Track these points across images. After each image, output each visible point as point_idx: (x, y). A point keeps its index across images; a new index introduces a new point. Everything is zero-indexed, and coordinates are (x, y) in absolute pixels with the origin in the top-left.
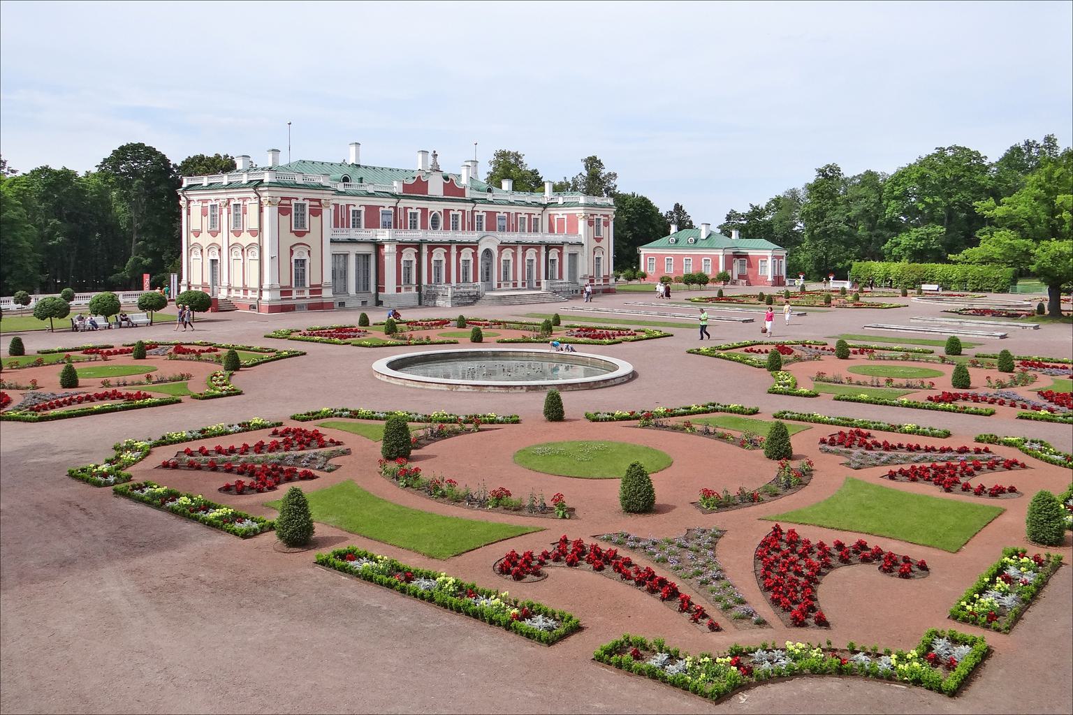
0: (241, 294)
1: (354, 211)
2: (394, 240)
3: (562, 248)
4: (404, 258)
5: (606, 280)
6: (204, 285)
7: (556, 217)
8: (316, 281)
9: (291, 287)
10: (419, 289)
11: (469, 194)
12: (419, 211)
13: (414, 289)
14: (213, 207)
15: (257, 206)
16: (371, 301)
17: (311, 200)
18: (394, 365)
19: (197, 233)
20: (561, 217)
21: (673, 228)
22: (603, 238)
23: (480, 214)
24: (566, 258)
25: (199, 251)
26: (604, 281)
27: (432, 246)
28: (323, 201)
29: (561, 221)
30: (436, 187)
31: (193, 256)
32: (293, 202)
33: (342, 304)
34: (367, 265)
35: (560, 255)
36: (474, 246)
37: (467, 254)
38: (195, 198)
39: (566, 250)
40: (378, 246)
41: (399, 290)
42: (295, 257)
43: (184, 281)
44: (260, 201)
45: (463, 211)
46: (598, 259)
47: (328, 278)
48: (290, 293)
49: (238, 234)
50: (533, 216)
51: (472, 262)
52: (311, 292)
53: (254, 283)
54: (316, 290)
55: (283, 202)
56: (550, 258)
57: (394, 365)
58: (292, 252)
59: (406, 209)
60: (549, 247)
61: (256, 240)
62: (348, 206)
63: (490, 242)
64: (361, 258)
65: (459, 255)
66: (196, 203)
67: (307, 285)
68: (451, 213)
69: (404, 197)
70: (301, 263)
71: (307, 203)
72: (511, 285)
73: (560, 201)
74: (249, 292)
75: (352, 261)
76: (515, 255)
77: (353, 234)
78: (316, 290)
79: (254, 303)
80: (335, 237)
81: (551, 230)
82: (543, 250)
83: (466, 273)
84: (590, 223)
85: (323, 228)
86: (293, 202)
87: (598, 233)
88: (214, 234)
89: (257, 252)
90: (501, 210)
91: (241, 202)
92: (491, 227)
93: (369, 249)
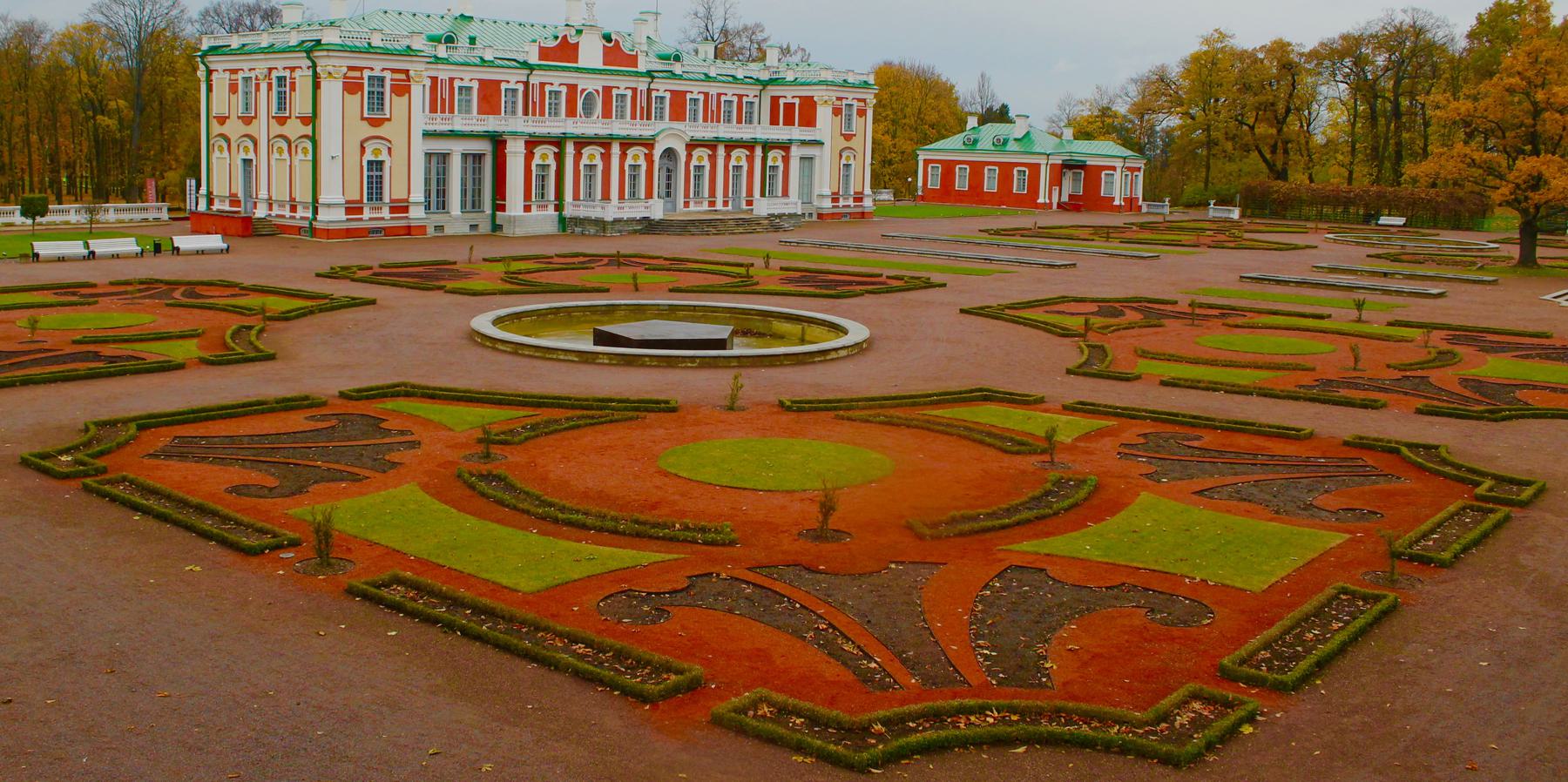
0: (287, 213)
1: (461, 88)
2: (522, 134)
4: (537, 161)
5: (859, 198)
6: (234, 201)
7: (782, 101)
8: (400, 194)
9: (361, 201)
10: (559, 208)
11: (642, 66)
12: (564, 90)
13: (551, 208)
14: (246, 80)
15: (310, 81)
16: (485, 228)
17: (394, 71)
18: (497, 322)
19: (222, 120)
20: (790, 100)
21: (972, 122)
23: (660, 94)
24: (795, 164)
25: (225, 145)
26: (856, 200)
27: (581, 143)
28: (412, 73)
29: (789, 107)
30: (591, 53)
31: (216, 154)
32: (366, 74)
33: (439, 228)
34: (478, 171)
35: (786, 160)
36: (648, 144)
37: (636, 155)
38: (220, 67)
39: (795, 152)
40: (498, 142)
41: (527, 208)
42: (369, 156)
43: (203, 190)
44: (315, 73)
46: (847, 166)
47: (418, 195)
48: (360, 210)
49: (282, 121)
50: (745, 99)
51: (644, 168)
52: (393, 210)
53: (303, 194)
54: (400, 207)
55: (351, 74)
56: (770, 163)
57: (497, 322)
58: (363, 149)
59: (542, 85)
60: (768, 146)
61: (308, 130)
62: (452, 80)
63: (670, 134)
64: (470, 160)
66: (222, 75)
67: (386, 199)
68: (615, 92)
69: (540, 67)
70: (376, 165)
71: (388, 75)
72: (705, 207)
73: (790, 78)
74: (299, 208)
75: (456, 165)
76: (713, 159)
77: (459, 123)
78: (400, 207)
79: (306, 224)
80: (431, 128)
81: (774, 121)
82: (759, 151)
83: (634, 186)
84: (837, 111)
85: (413, 115)
86: (366, 74)
87: (849, 126)
88: (247, 121)
89: (309, 145)
90: (695, 91)
91: (287, 73)
92: (678, 114)
93: (484, 147)
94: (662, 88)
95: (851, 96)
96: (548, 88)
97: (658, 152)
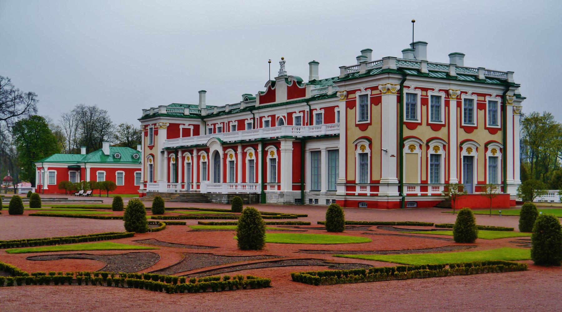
3: (280, 143)
11: (308, 96)
12: (270, 119)
22: (370, 124)
45: (304, 111)
59: (261, 118)
60: (265, 142)
62: (229, 122)
65: (183, 158)
69: (259, 108)
84: (350, 105)
94: (318, 107)
95: (362, 87)
96: (264, 120)
97: (211, 154)
